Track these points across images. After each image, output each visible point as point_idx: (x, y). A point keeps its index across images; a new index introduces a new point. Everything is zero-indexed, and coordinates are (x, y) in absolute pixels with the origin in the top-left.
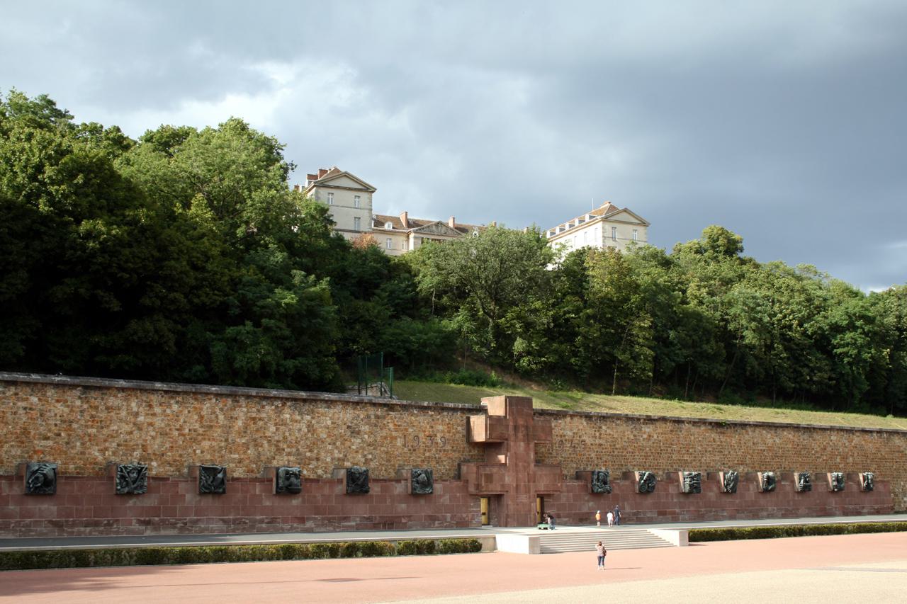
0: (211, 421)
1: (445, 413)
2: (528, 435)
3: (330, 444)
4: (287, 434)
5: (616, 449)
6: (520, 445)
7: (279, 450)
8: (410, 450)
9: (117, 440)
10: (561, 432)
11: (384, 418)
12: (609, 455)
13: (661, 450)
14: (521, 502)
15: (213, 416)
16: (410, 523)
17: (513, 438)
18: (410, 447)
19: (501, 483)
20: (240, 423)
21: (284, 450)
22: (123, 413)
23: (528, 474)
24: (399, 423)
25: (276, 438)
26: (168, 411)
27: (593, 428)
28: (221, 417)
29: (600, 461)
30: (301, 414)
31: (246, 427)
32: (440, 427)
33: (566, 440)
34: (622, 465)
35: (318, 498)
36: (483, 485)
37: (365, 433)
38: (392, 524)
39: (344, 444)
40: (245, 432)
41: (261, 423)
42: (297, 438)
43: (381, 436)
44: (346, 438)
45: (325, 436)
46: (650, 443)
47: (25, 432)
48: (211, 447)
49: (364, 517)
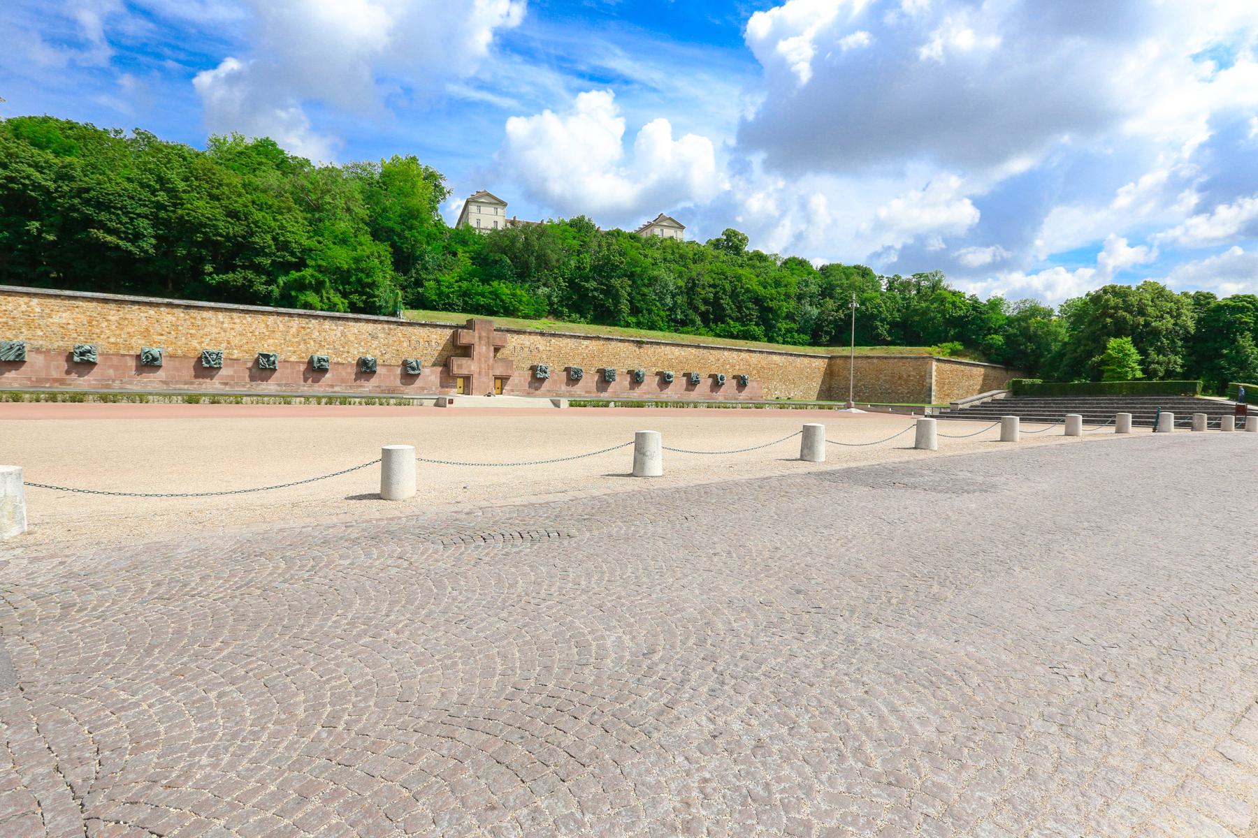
0: (274, 328)
9: (210, 337)
11: (395, 329)
15: (276, 325)
17: (478, 343)
20: (294, 330)
22: (213, 322)
26: (244, 322)
28: (281, 326)
31: (299, 332)
41: (309, 330)
47: (147, 330)
48: (274, 343)
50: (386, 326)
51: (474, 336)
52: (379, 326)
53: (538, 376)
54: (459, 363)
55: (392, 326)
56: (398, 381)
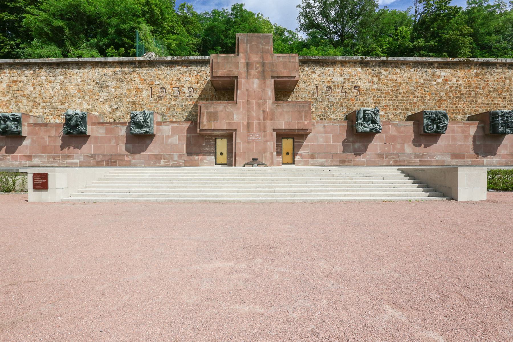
1: (194, 67)
2: (264, 71)
3: (79, 98)
4: (43, 91)
5: (399, 93)
6: (253, 83)
7: (36, 105)
8: (155, 100)
10: (329, 78)
12: (389, 100)
13: (462, 94)
14: (253, 140)
16: (134, 161)
17: (244, 75)
18: (156, 97)
19: (228, 121)
21: (39, 104)
23: (264, 112)
24: (146, 78)
25: (34, 95)
27: (371, 73)
29: (378, 105)
30: (55, 75)
31: (9, 87)
32: (188, 79)
33: (335, 86)
34: (407, 110)
35: (46, 139)
36: (205, 123)
37: (113, 88)
38: (115, 162)
39: (92, 98)
40: (8, 92)
41: (21, 84)
42: (51, 94)
43: (128, 90)
44: (94, 92)
45: (75, 92)
46: (447, 87)
49: (87, 155)
50: (118, 70)
51: (237, 64)
52: (109, 71)
53: (360, 129)
54: (211, 110)
55: (126, 70)
56: (122, 148)
